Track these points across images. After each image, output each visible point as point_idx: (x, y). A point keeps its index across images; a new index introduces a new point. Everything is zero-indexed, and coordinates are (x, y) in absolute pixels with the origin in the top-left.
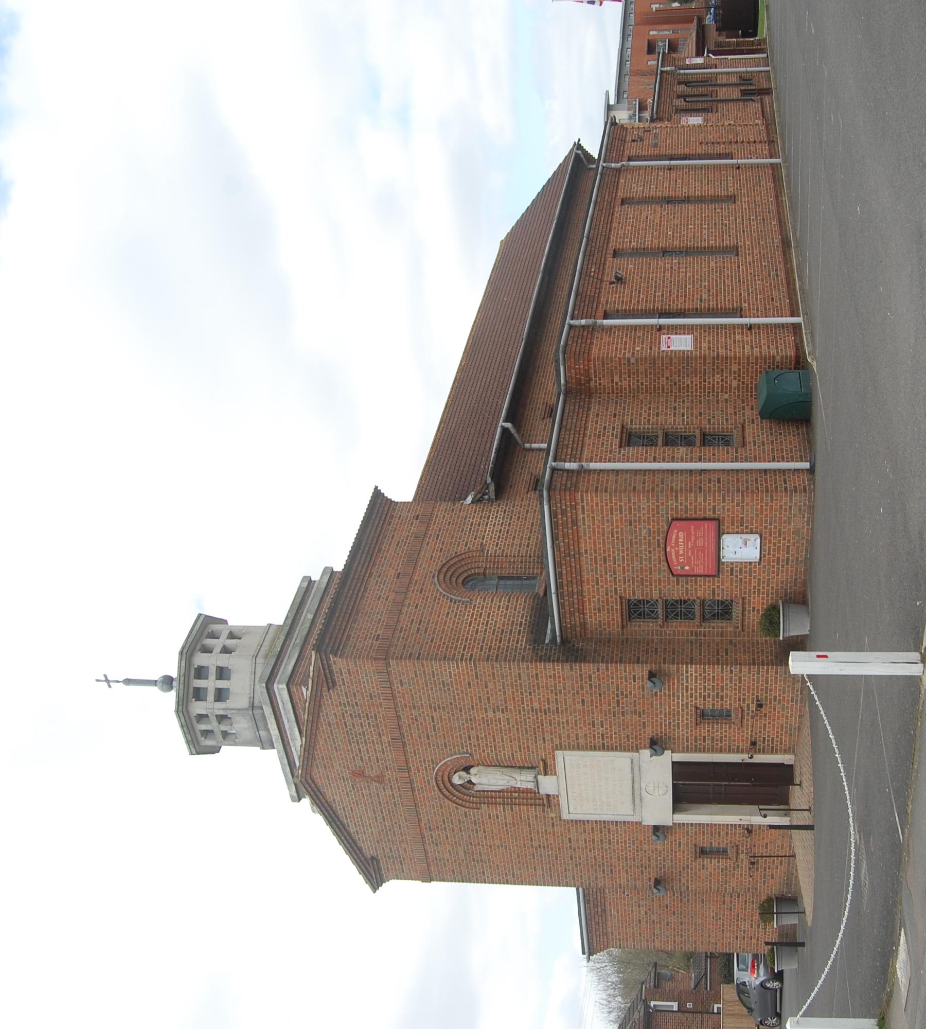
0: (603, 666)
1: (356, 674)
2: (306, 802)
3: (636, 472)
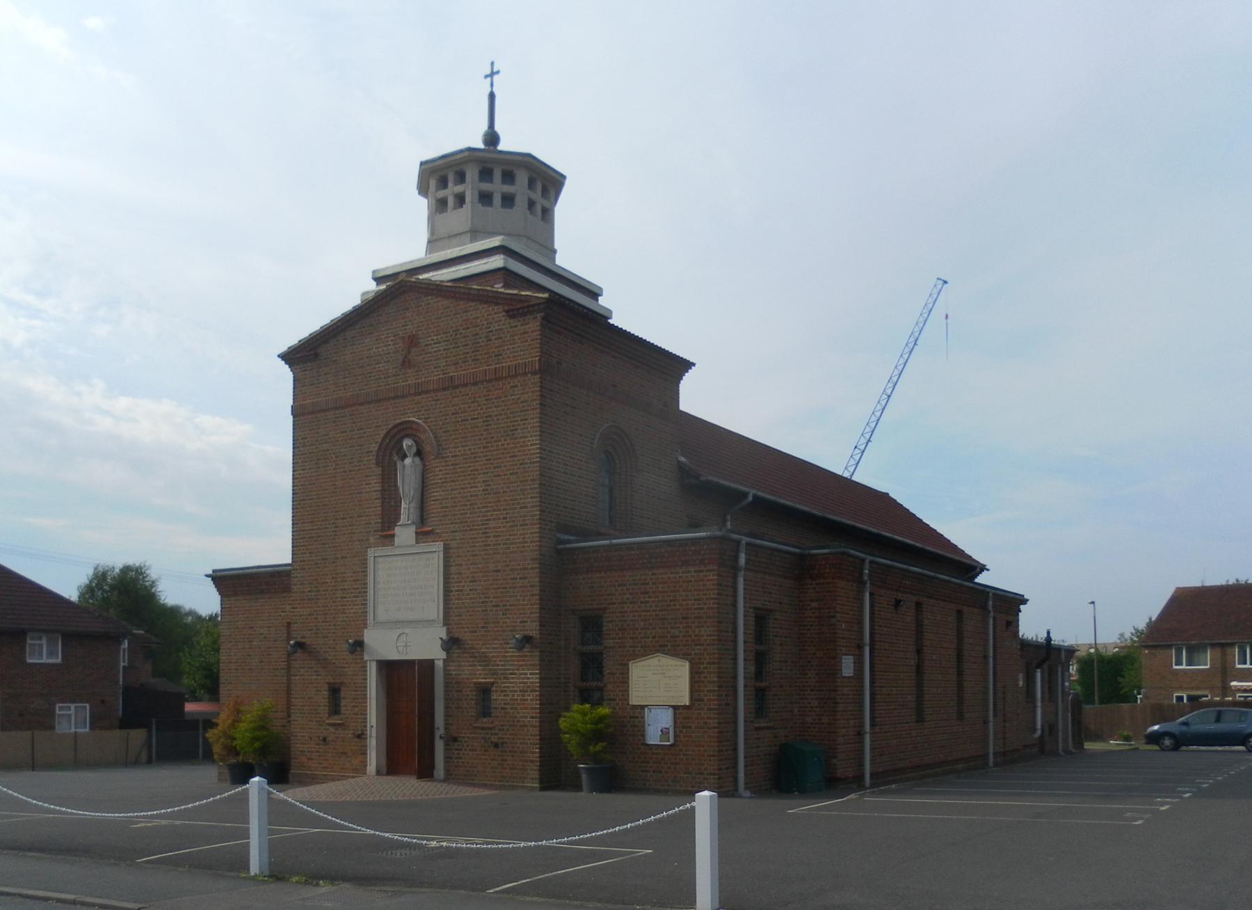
0: (536, 591)
1: (523, 342)
2: (372, 286)
3: (735, 624)
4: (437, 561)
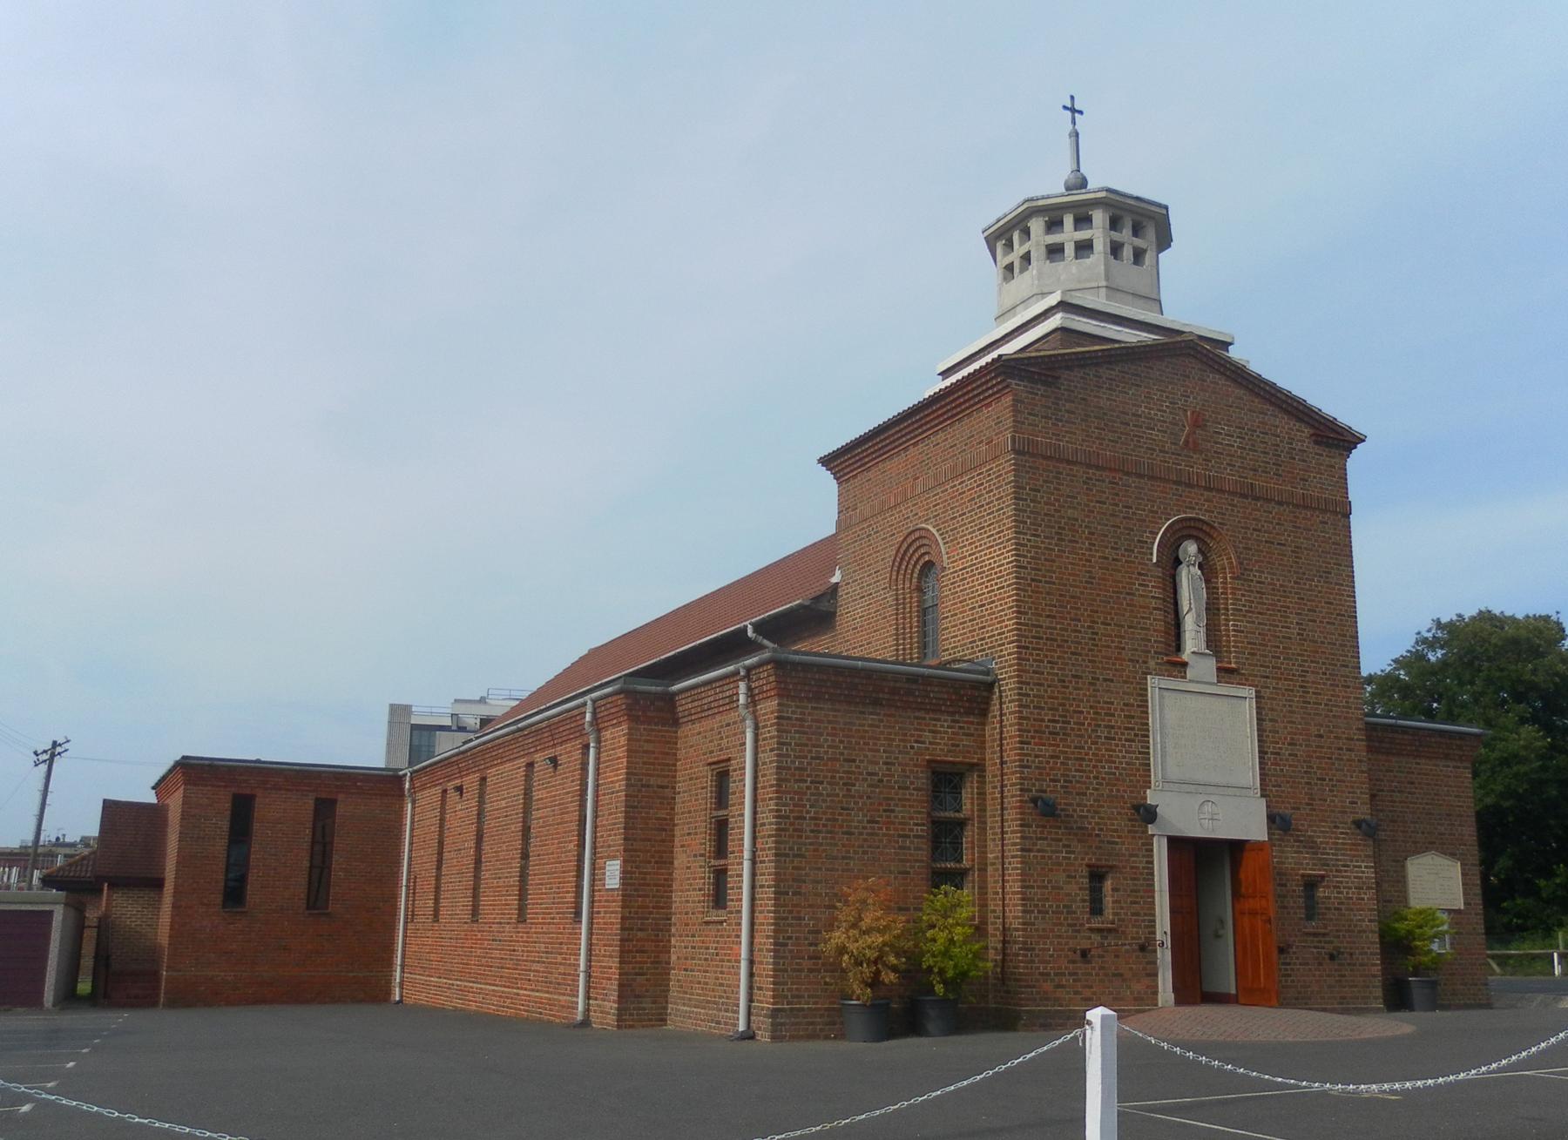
4: (1248, 709)
